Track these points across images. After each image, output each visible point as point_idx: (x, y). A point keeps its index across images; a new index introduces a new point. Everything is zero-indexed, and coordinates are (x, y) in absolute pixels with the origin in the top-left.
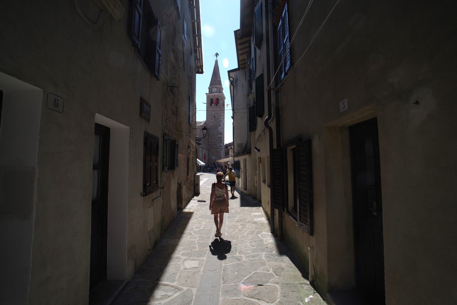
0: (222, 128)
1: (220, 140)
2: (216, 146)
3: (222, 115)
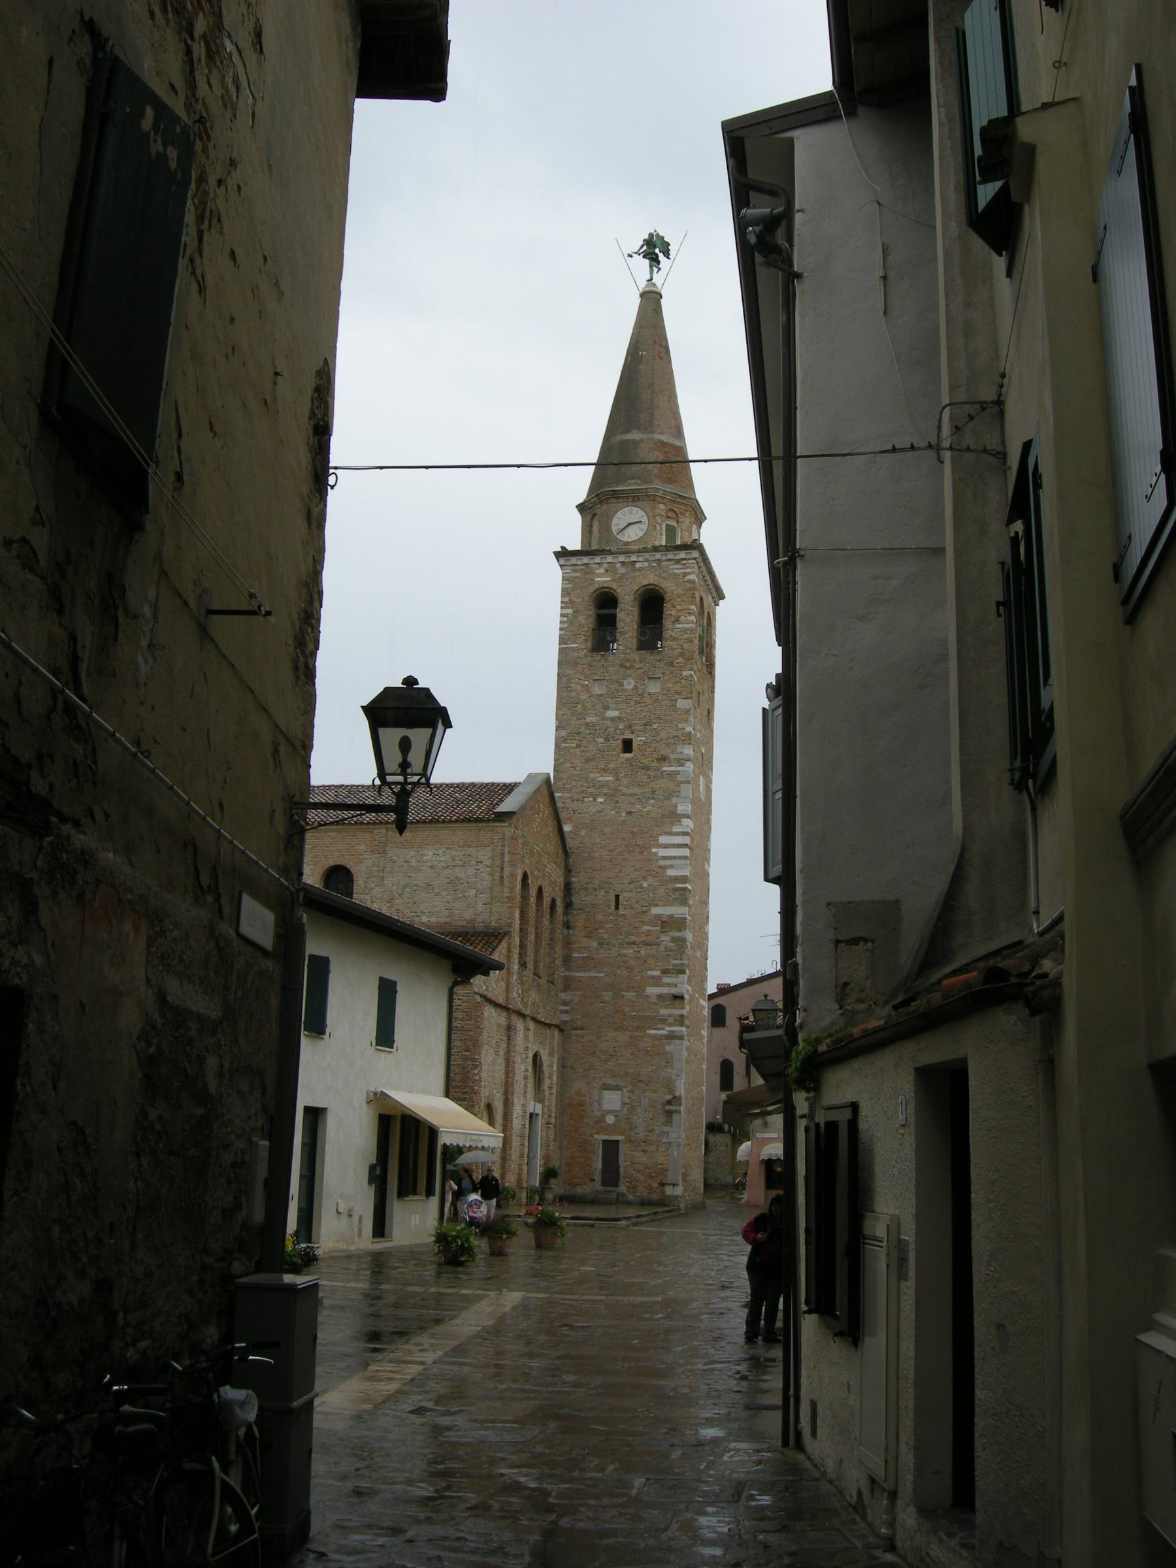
0: (686, 840)
1: (667, 949)
2: (630, 995)
3: (689, 729)
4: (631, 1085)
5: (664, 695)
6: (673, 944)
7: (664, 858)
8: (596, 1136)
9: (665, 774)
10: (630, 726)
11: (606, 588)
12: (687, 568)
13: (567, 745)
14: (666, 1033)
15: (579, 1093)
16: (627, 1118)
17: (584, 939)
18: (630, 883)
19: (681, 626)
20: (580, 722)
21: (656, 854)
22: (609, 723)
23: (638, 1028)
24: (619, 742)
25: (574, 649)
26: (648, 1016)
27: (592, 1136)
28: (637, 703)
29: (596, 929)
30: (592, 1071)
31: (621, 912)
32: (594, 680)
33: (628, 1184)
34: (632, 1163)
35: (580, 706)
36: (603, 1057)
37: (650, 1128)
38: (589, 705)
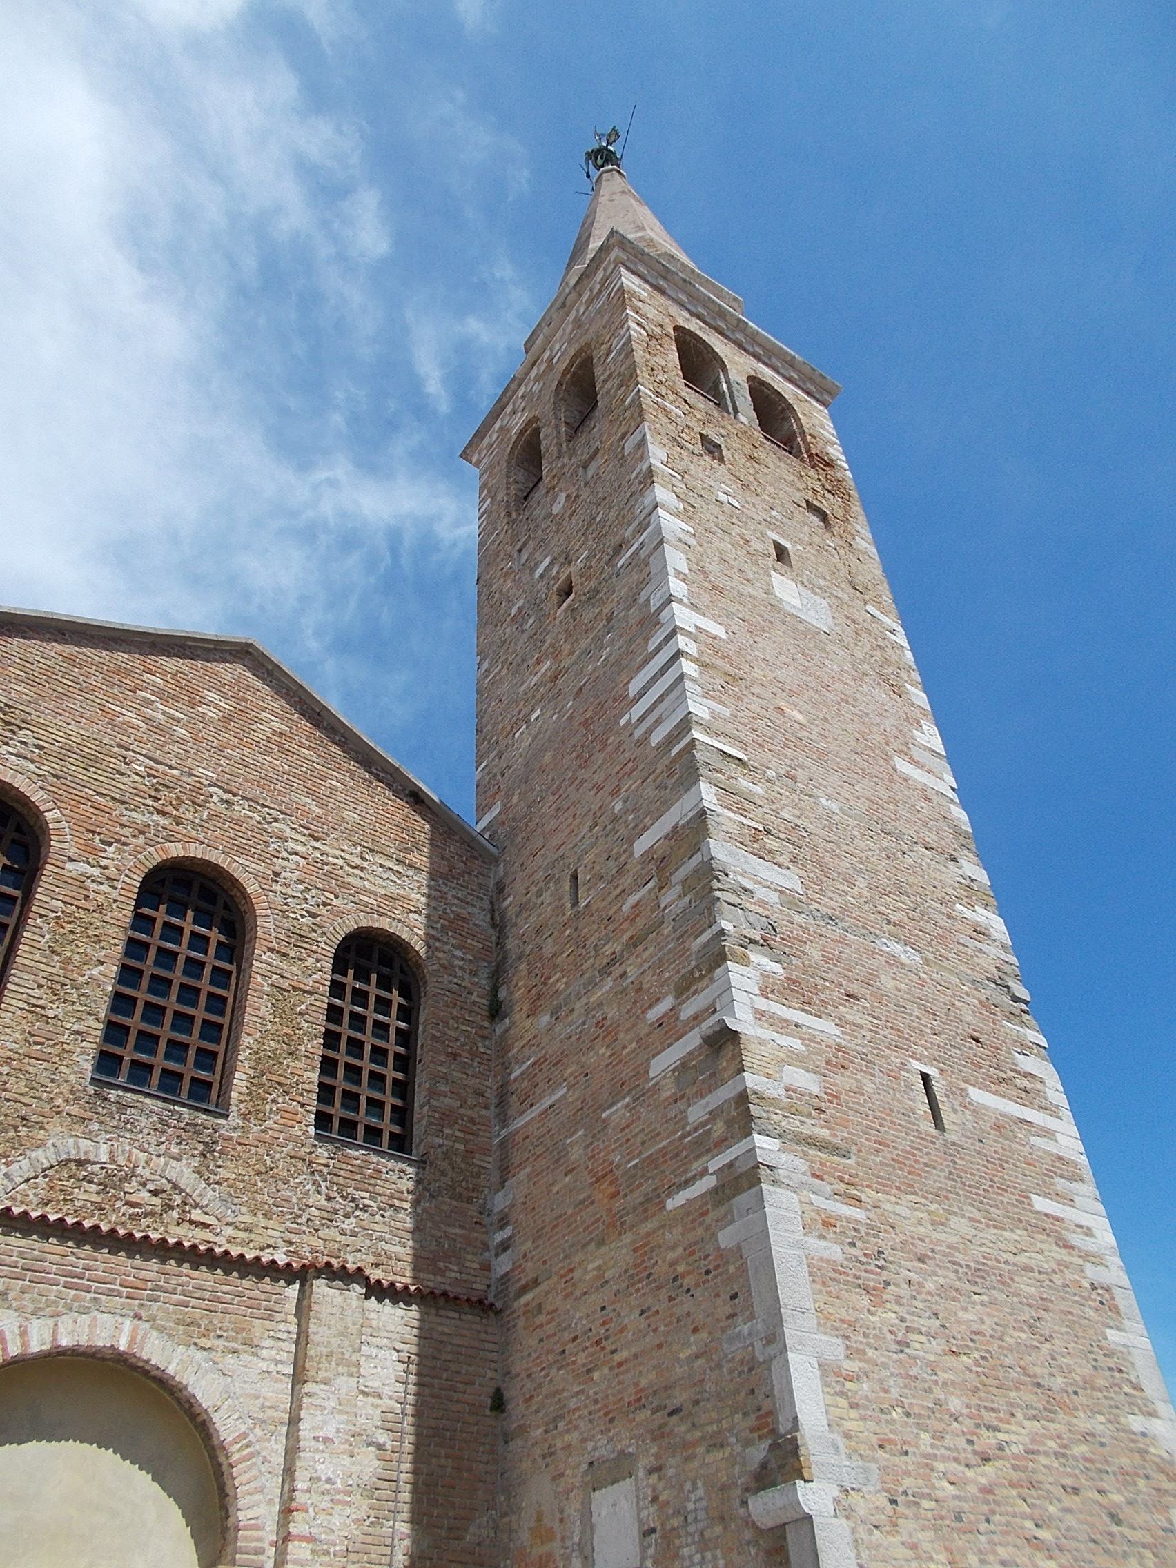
2: (616, 1113)
4: (654, 1440)
7: (642, 719)
9: (622, 570)
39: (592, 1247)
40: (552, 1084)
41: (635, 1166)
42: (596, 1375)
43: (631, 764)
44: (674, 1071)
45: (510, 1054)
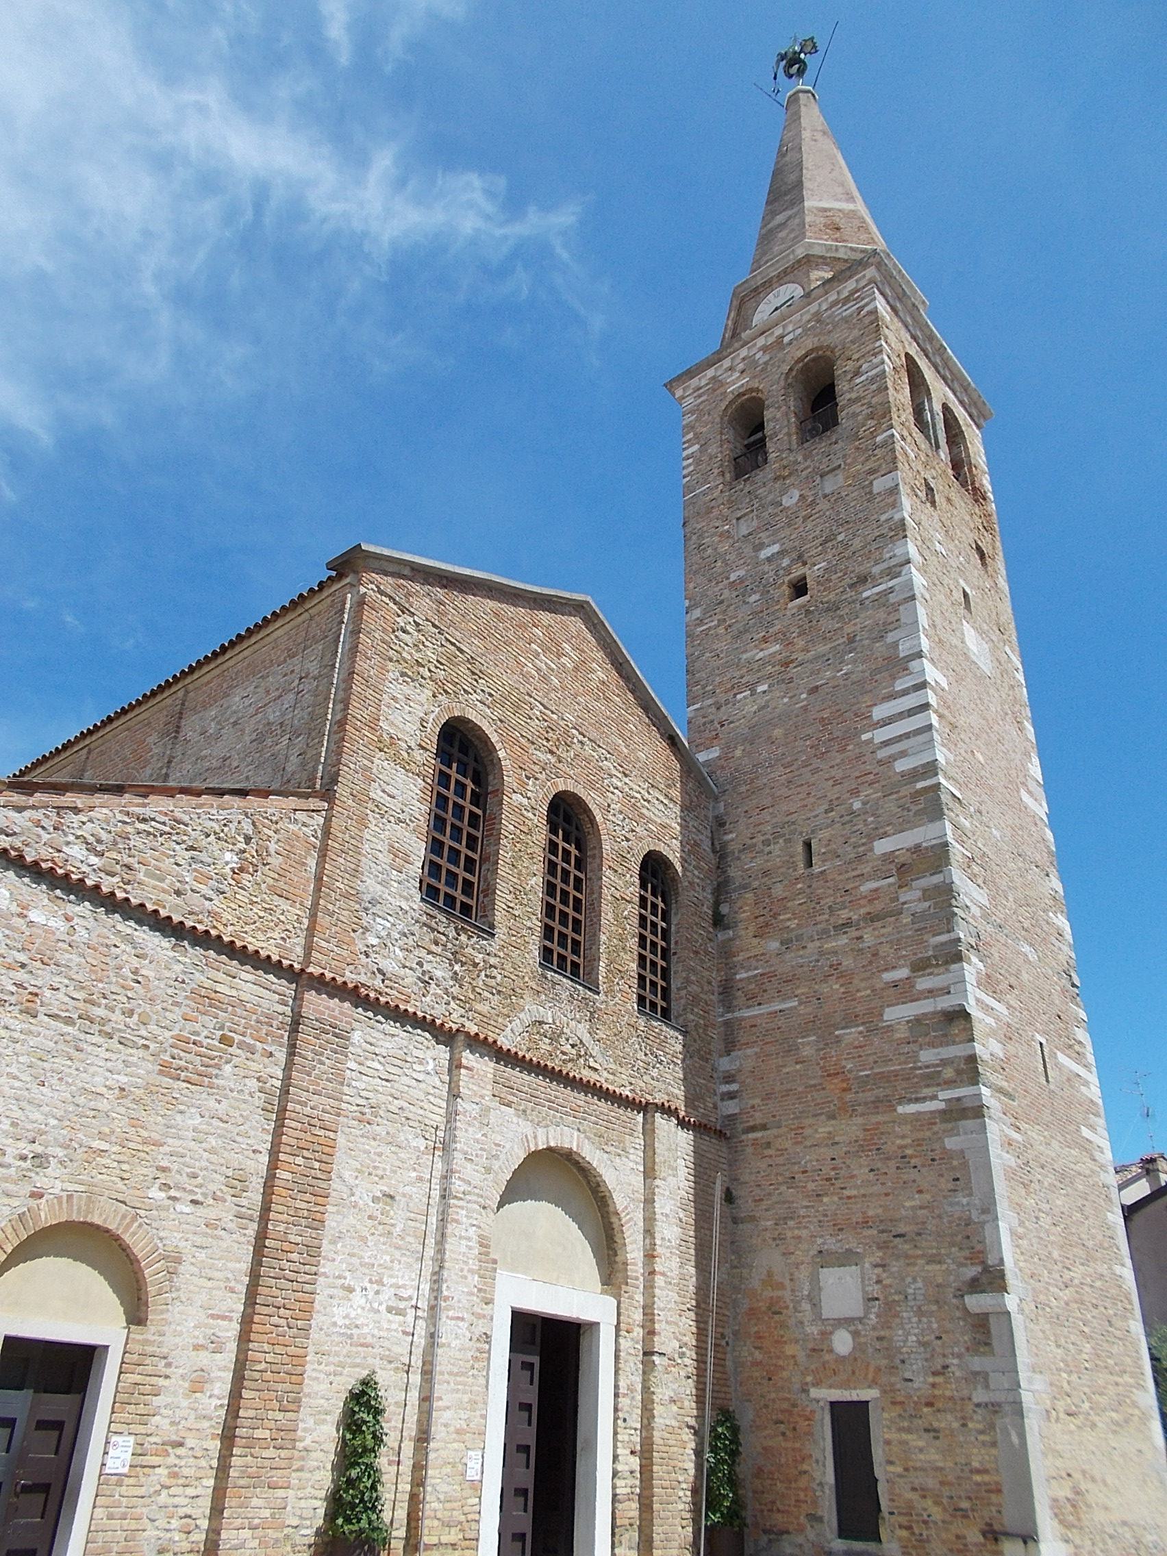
2: (852, 1034)
4: (879, 1248)
5: (850, 485)
6: (927, 904)
7: (886, 743)
8: (814, 1393)
9: (867, 602)
10: (800, 557)
11: (743, 394)
12: (863, 299)
13: (705, 627)
14: (942, 1106)
15: (769, 1280)
16: (880, 1339)
17: (755, 941)
18: (826, 812)
19: (863, 378)
20: (721, 586)
21: (871, 741)
22: (766, 568)
23: (878, 1104)
24: (785, 587)
25: (704, 494)
26: (896, 1074)
27: (806, 1391)
28: (806, 518)
29: (775, 916)
30: (791, 1223)
31: (816, 869)
32: (738, 519)
33: (904, 1533)
34: (906, 1470)
35: (719, 564)
36: (811, 1186)
37: (939, 1363)
38: (732, 557)
39: (823, 1117)
40: (782, 995)
41: (867, 1076)
42: (825, 1200)
43: (872, 777)
44: (908, 1022)
45: (735, 959)
